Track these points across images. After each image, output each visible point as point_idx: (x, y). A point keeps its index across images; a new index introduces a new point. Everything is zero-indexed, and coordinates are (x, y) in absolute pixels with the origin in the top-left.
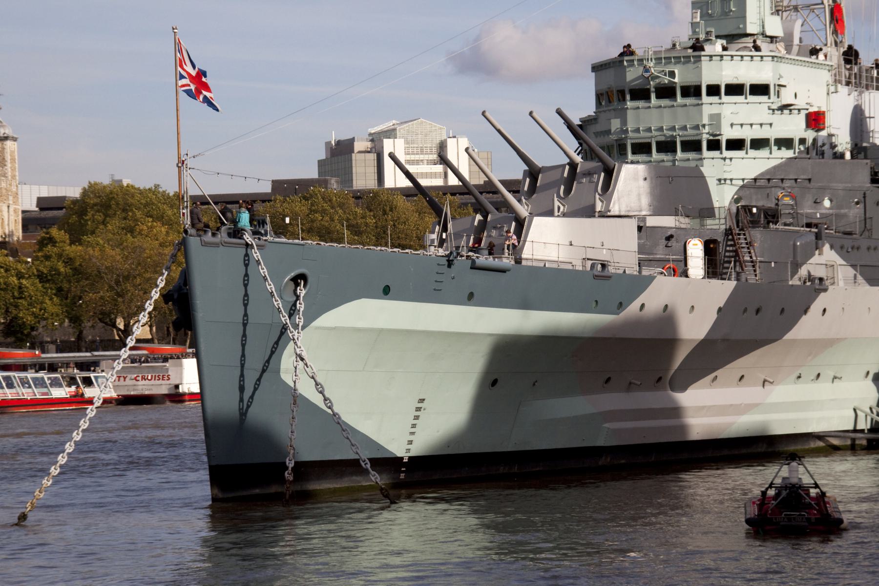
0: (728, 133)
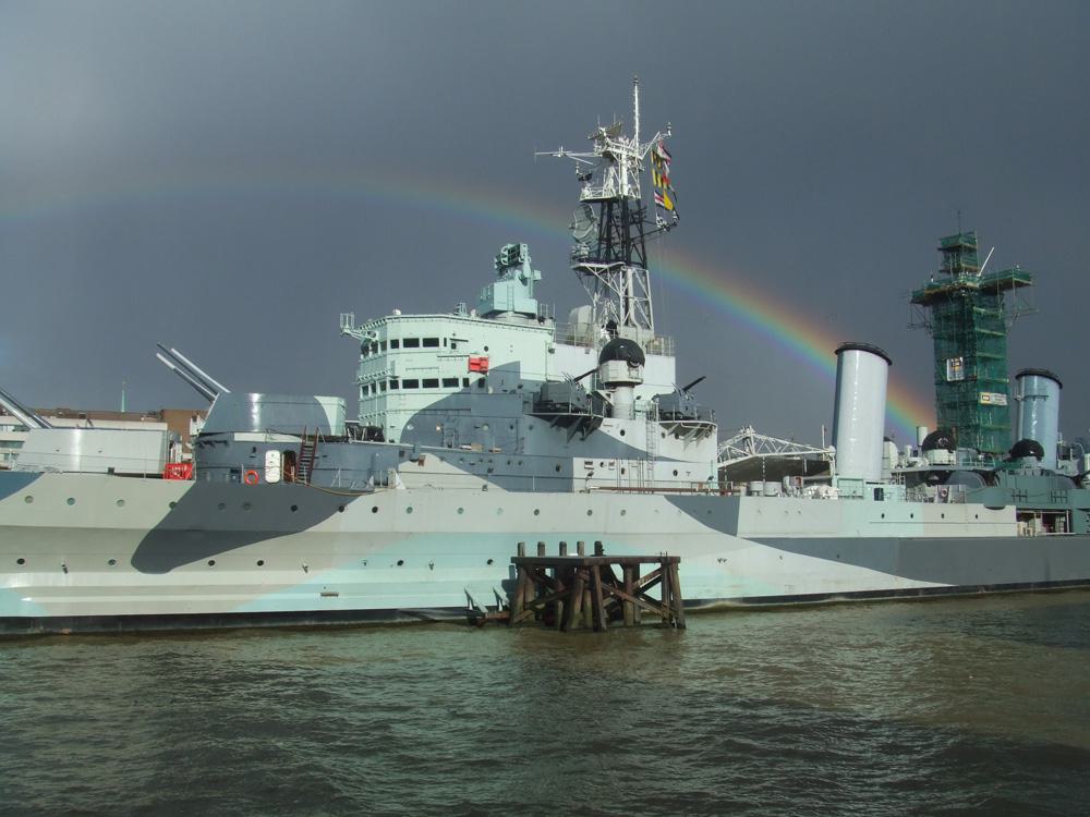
0: (403, 375)
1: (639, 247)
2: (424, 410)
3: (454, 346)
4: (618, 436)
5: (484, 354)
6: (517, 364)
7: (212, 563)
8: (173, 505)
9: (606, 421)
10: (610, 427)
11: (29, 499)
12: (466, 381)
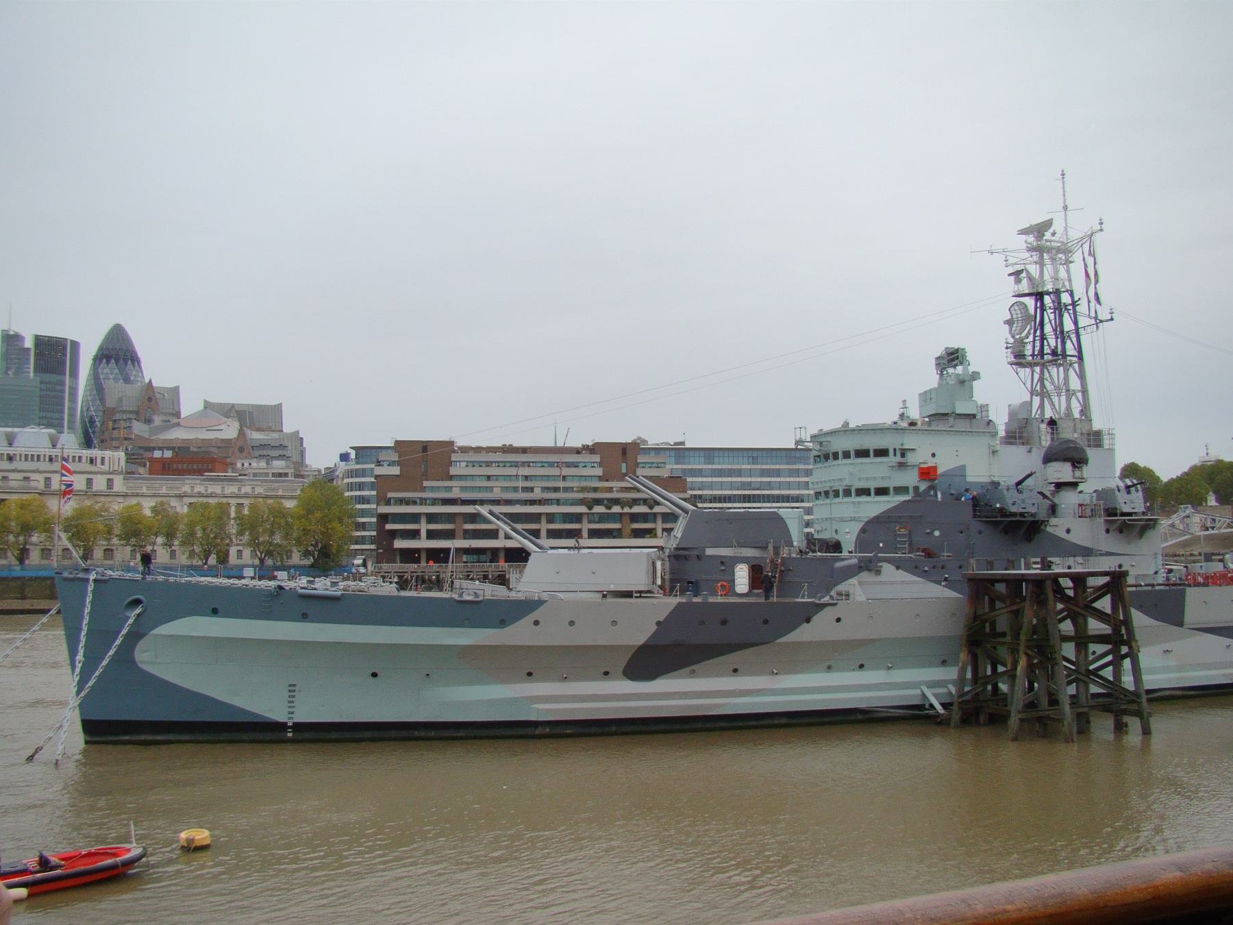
1: (1073, 336)
2: (877, 517)
3: (903, 455)
4: (1061, 533)
5: (931, 462)
6: (963, 468)
7: (694, 671)
8: (658, 623)
9: (1053, 521)
10: (1057, 527)
11: (536, 623)
12: (916, 488)
